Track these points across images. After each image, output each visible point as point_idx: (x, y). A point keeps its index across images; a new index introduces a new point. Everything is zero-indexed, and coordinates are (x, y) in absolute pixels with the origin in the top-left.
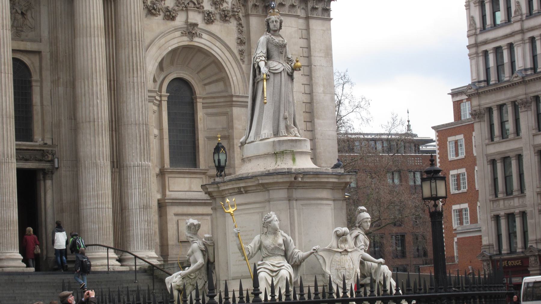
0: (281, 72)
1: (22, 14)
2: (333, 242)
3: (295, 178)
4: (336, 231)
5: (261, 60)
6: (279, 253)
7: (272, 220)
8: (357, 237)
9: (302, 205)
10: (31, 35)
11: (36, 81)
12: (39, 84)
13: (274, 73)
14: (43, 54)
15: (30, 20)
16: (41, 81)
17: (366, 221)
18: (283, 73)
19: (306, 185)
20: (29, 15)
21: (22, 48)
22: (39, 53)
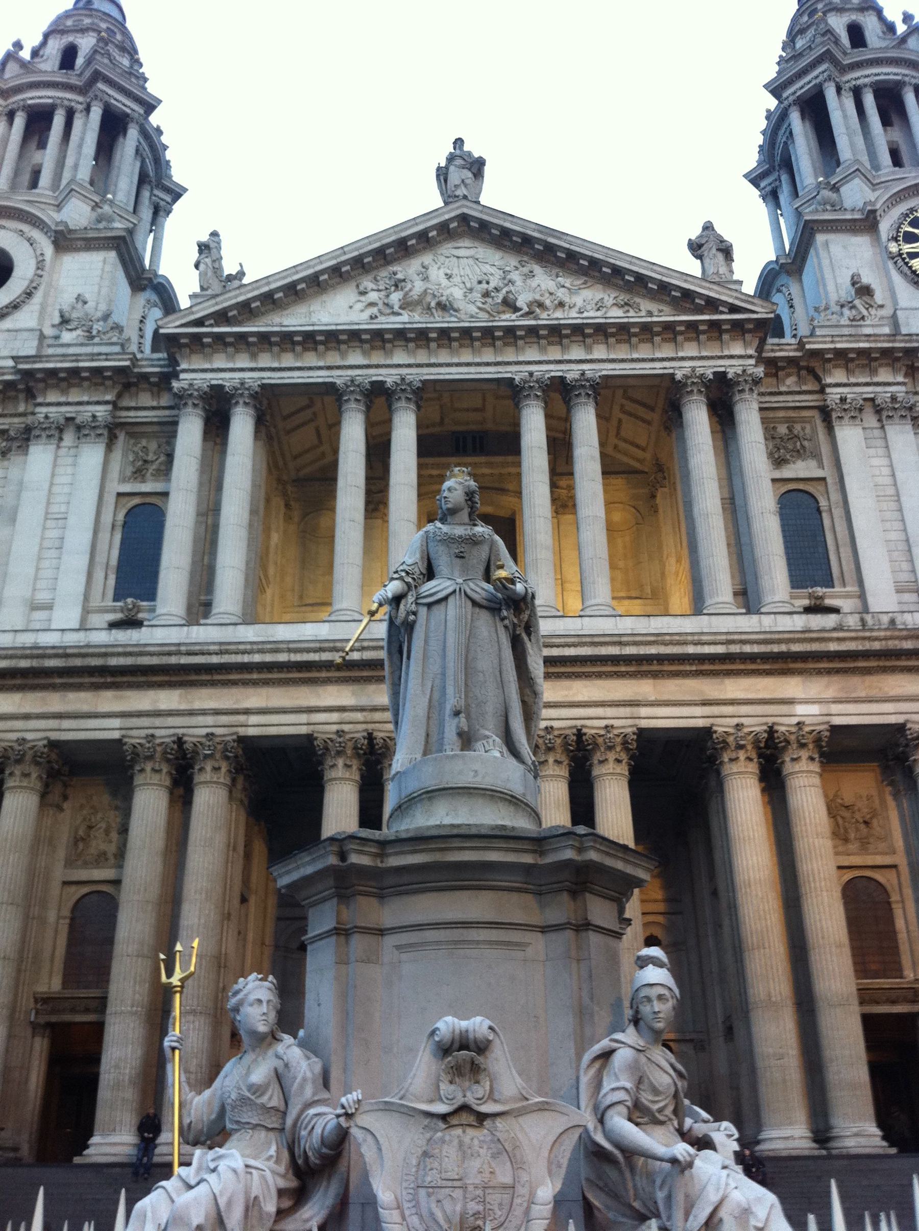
0: (445, 599)
1: (866, 823)
2: (421, 1078)
3: (343, 856)
4: (433, 1033)
5: (392, 579)
6: (254, 1121)
7: (241, 1003)
8: (607, 1055)
9: (398, 947)
10: (882, 846)
11: (897, 902)
12: (900, 905)
13: (429, 606)
14: (900, 868)
15: (878, 829)
16: (903, 902)
17: (649, 999)
18: (451, 600)
19: (406, 879)
20: (875, 822)
21: (870, 863)
22: (895, 866)
